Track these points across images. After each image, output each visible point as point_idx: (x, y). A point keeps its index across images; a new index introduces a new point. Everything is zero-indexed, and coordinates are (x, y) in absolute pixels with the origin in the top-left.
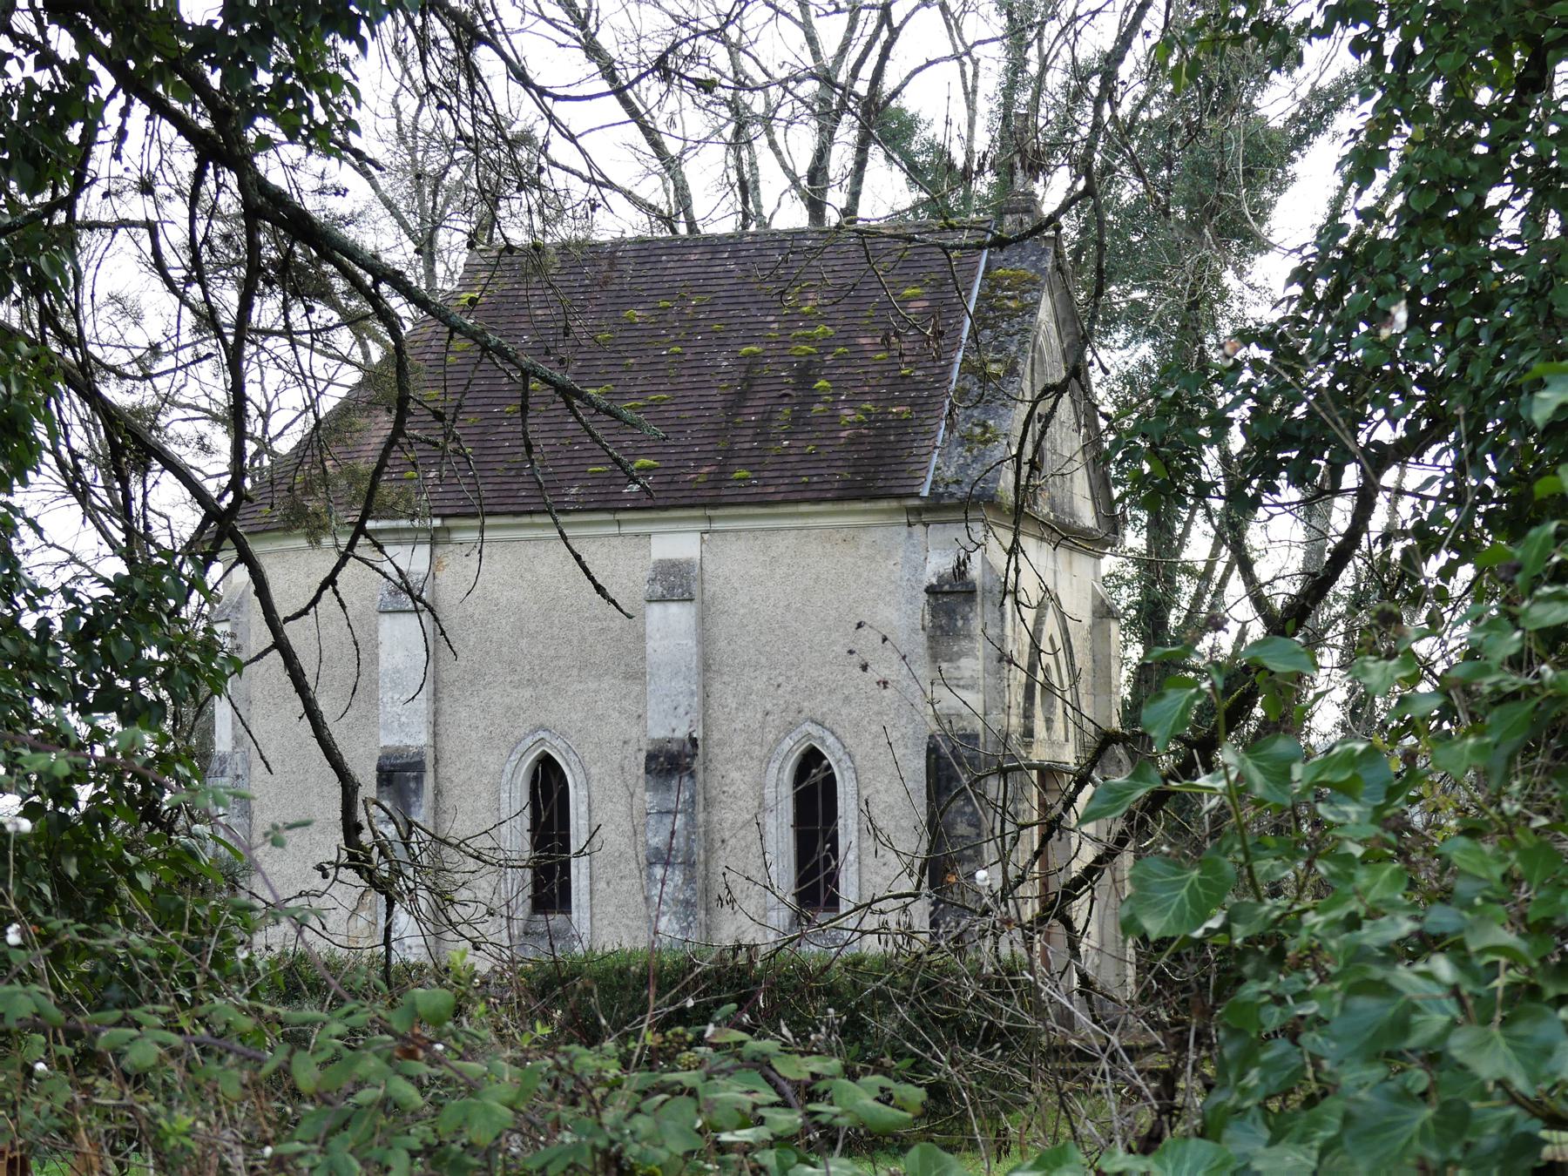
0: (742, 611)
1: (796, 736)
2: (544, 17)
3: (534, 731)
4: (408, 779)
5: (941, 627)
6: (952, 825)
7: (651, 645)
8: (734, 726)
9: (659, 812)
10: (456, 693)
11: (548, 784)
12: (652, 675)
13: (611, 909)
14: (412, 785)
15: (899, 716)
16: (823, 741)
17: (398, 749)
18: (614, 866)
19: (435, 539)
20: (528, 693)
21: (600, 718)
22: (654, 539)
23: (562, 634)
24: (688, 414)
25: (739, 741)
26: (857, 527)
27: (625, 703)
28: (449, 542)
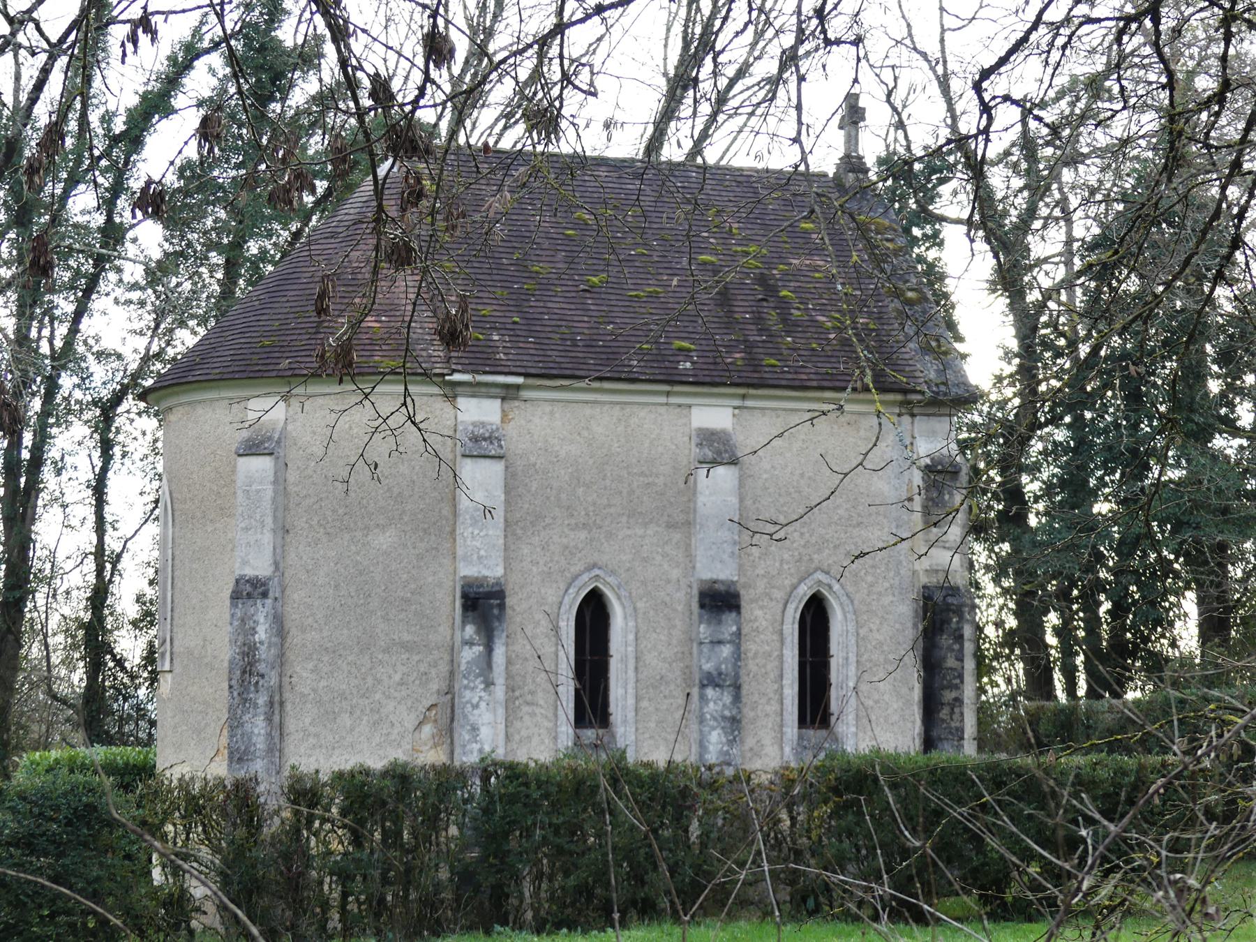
0: (765, 476)
1: (809, 582)
2: (915, 49)
3: (590, 568)
4: (492, 607)
5: (932, 500)
6: (944, 658)
7: (701, 499)
8: (757, 572)
9: (712, 642)
10: (519, 532)
11: (593, 616)
12: (702, 526)
13: (652, 725)
14: (496, 611)
15: (888, 570)
16: (830, 587)
17: (477, 578)
18: (655, 687)
19: (508, 394)
20: (583, 535)
21: (645, 560)
22: (694, 410)
23: (614, 486)
24: (613, 297)
25: (761, 585)
26: (860, 414)
27: (667, 548)
28: (516, 399)
